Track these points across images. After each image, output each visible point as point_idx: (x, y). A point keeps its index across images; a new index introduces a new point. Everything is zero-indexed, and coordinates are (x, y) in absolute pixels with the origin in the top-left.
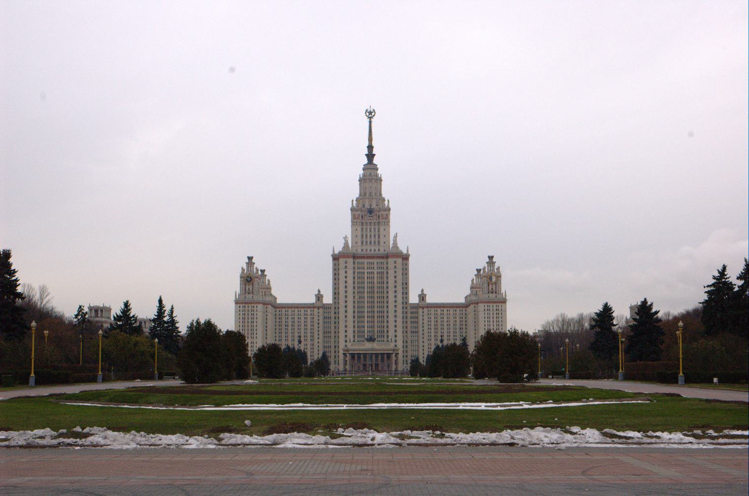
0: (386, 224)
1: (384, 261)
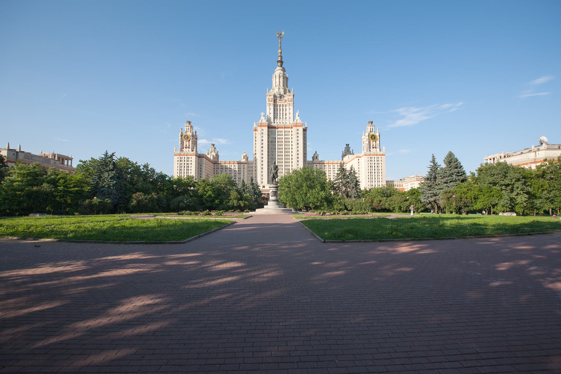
0: (291, 105)
1: (290, 130)
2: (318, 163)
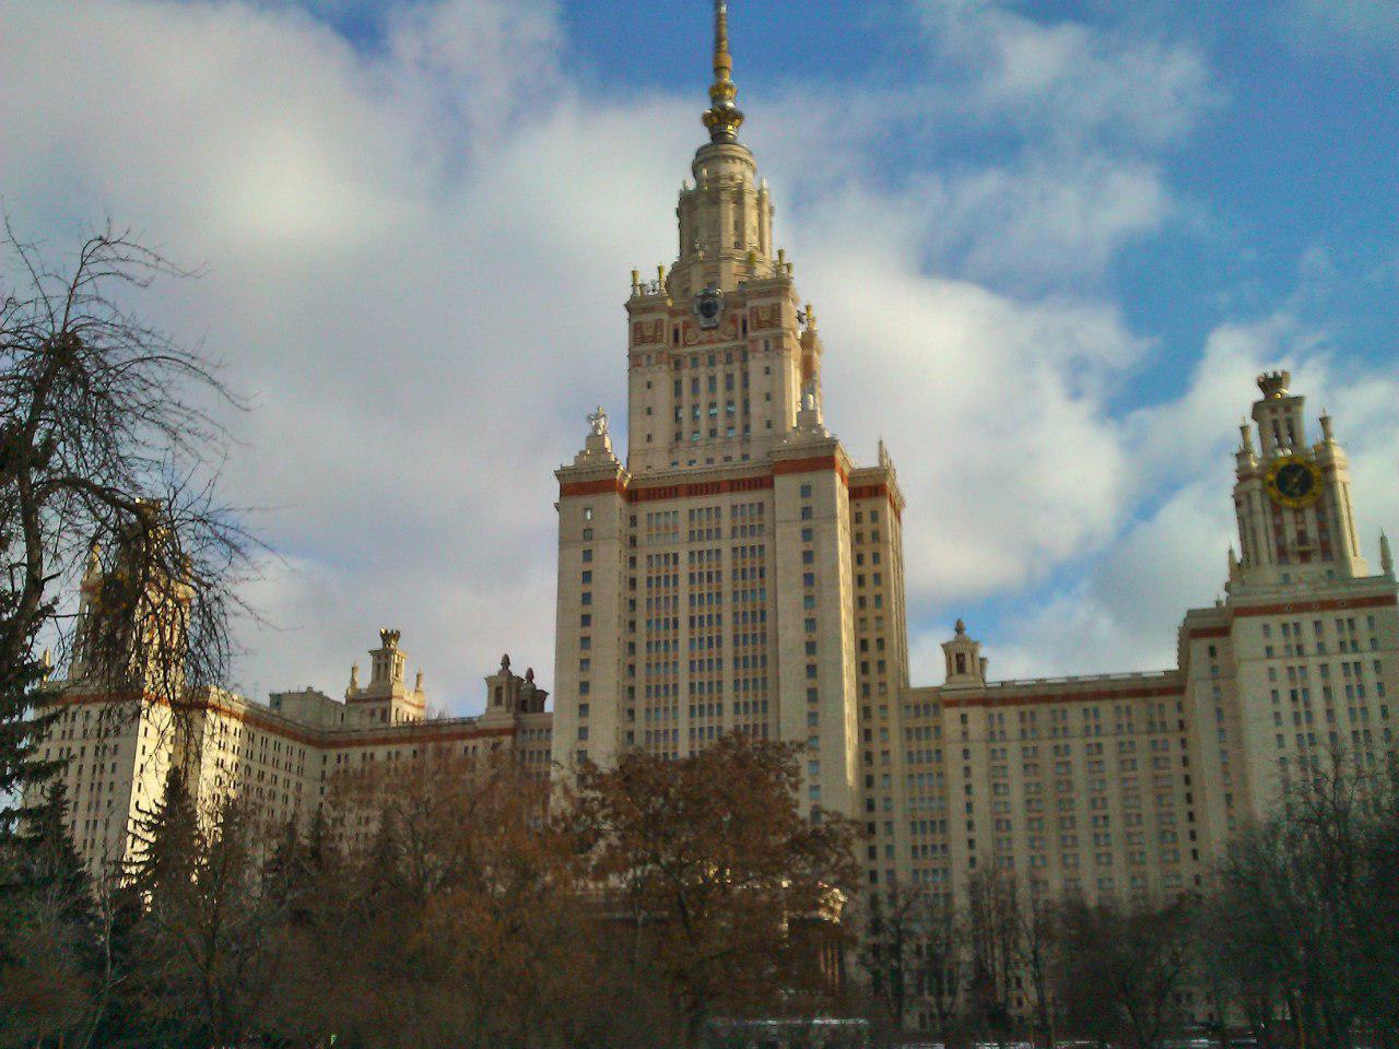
0: (771, 348)
2: (971, 702)
